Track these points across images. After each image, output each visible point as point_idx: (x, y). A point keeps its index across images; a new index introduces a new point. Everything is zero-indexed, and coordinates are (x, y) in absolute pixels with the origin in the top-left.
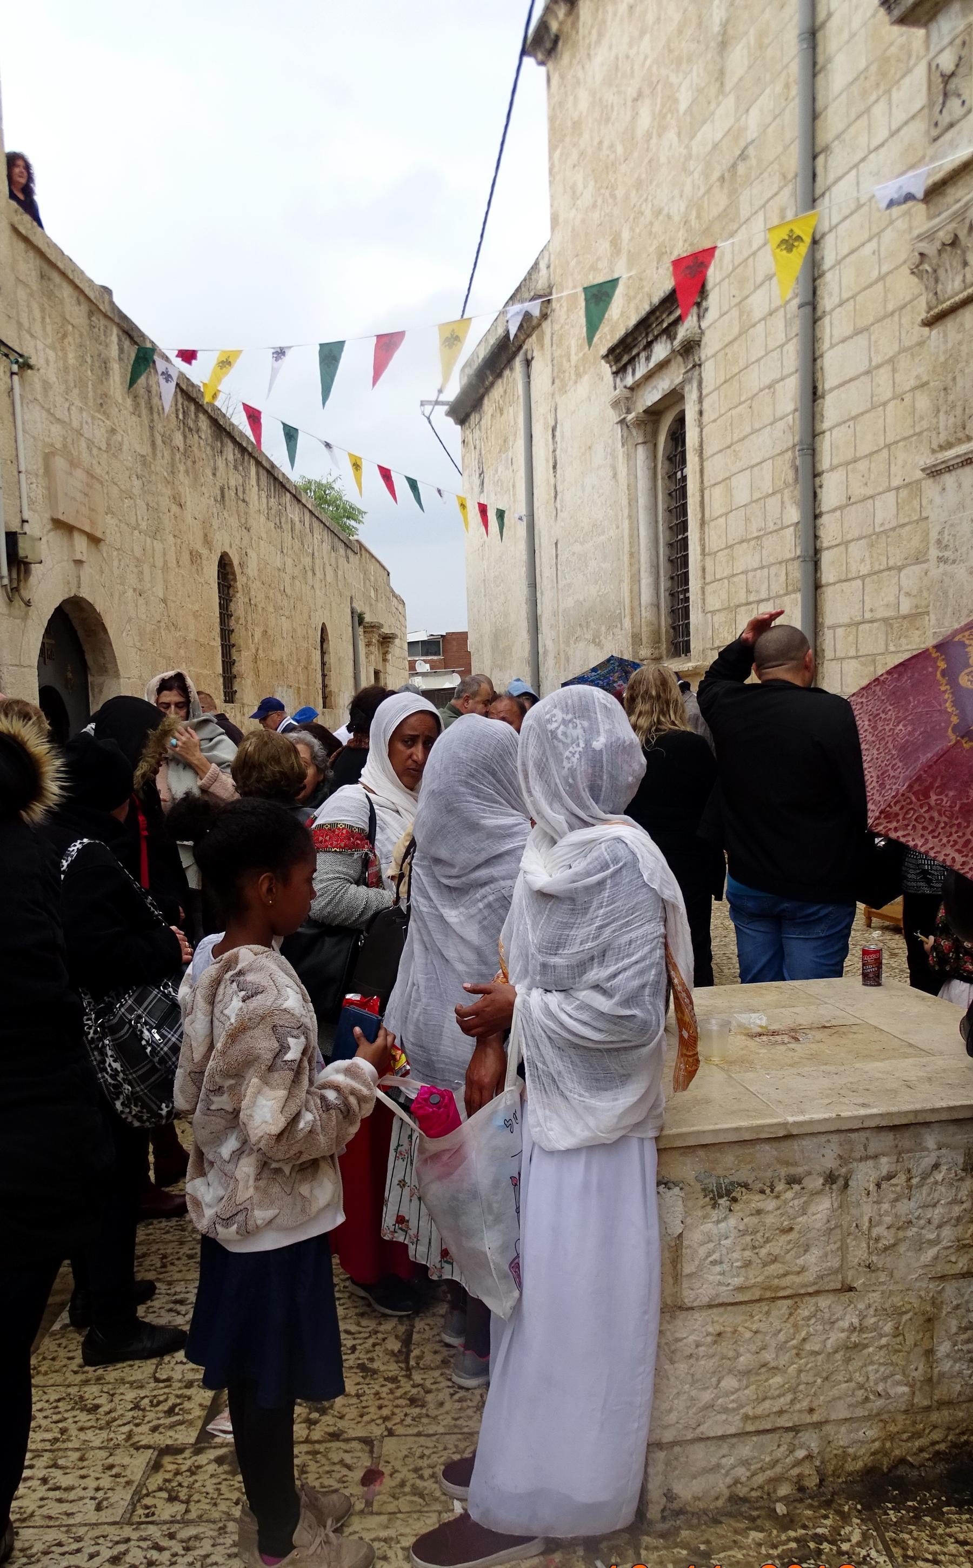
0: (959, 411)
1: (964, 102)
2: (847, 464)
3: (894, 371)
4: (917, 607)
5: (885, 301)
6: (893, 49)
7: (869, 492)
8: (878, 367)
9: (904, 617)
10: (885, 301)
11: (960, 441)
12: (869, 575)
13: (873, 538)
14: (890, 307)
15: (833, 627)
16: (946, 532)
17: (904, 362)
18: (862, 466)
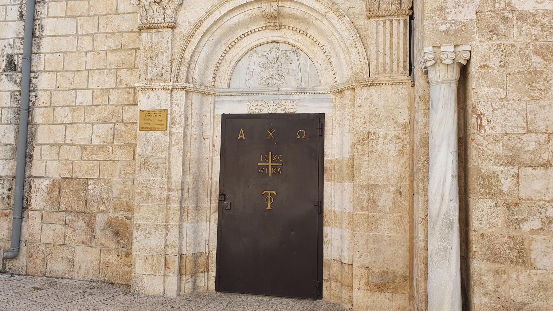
0: (159, 68)
2: (57, 72)
3: (93, 40)
4: (104, 142)
5: (89, 9)
7: (72, 87)
8: (82, 35)
9: (95, 145)
10: (89, 9)
12: (71, 124)
13: (74, 108)
14: (92, 13)
15: (41, 144)
17: (100, 37)
18: (70, 75)
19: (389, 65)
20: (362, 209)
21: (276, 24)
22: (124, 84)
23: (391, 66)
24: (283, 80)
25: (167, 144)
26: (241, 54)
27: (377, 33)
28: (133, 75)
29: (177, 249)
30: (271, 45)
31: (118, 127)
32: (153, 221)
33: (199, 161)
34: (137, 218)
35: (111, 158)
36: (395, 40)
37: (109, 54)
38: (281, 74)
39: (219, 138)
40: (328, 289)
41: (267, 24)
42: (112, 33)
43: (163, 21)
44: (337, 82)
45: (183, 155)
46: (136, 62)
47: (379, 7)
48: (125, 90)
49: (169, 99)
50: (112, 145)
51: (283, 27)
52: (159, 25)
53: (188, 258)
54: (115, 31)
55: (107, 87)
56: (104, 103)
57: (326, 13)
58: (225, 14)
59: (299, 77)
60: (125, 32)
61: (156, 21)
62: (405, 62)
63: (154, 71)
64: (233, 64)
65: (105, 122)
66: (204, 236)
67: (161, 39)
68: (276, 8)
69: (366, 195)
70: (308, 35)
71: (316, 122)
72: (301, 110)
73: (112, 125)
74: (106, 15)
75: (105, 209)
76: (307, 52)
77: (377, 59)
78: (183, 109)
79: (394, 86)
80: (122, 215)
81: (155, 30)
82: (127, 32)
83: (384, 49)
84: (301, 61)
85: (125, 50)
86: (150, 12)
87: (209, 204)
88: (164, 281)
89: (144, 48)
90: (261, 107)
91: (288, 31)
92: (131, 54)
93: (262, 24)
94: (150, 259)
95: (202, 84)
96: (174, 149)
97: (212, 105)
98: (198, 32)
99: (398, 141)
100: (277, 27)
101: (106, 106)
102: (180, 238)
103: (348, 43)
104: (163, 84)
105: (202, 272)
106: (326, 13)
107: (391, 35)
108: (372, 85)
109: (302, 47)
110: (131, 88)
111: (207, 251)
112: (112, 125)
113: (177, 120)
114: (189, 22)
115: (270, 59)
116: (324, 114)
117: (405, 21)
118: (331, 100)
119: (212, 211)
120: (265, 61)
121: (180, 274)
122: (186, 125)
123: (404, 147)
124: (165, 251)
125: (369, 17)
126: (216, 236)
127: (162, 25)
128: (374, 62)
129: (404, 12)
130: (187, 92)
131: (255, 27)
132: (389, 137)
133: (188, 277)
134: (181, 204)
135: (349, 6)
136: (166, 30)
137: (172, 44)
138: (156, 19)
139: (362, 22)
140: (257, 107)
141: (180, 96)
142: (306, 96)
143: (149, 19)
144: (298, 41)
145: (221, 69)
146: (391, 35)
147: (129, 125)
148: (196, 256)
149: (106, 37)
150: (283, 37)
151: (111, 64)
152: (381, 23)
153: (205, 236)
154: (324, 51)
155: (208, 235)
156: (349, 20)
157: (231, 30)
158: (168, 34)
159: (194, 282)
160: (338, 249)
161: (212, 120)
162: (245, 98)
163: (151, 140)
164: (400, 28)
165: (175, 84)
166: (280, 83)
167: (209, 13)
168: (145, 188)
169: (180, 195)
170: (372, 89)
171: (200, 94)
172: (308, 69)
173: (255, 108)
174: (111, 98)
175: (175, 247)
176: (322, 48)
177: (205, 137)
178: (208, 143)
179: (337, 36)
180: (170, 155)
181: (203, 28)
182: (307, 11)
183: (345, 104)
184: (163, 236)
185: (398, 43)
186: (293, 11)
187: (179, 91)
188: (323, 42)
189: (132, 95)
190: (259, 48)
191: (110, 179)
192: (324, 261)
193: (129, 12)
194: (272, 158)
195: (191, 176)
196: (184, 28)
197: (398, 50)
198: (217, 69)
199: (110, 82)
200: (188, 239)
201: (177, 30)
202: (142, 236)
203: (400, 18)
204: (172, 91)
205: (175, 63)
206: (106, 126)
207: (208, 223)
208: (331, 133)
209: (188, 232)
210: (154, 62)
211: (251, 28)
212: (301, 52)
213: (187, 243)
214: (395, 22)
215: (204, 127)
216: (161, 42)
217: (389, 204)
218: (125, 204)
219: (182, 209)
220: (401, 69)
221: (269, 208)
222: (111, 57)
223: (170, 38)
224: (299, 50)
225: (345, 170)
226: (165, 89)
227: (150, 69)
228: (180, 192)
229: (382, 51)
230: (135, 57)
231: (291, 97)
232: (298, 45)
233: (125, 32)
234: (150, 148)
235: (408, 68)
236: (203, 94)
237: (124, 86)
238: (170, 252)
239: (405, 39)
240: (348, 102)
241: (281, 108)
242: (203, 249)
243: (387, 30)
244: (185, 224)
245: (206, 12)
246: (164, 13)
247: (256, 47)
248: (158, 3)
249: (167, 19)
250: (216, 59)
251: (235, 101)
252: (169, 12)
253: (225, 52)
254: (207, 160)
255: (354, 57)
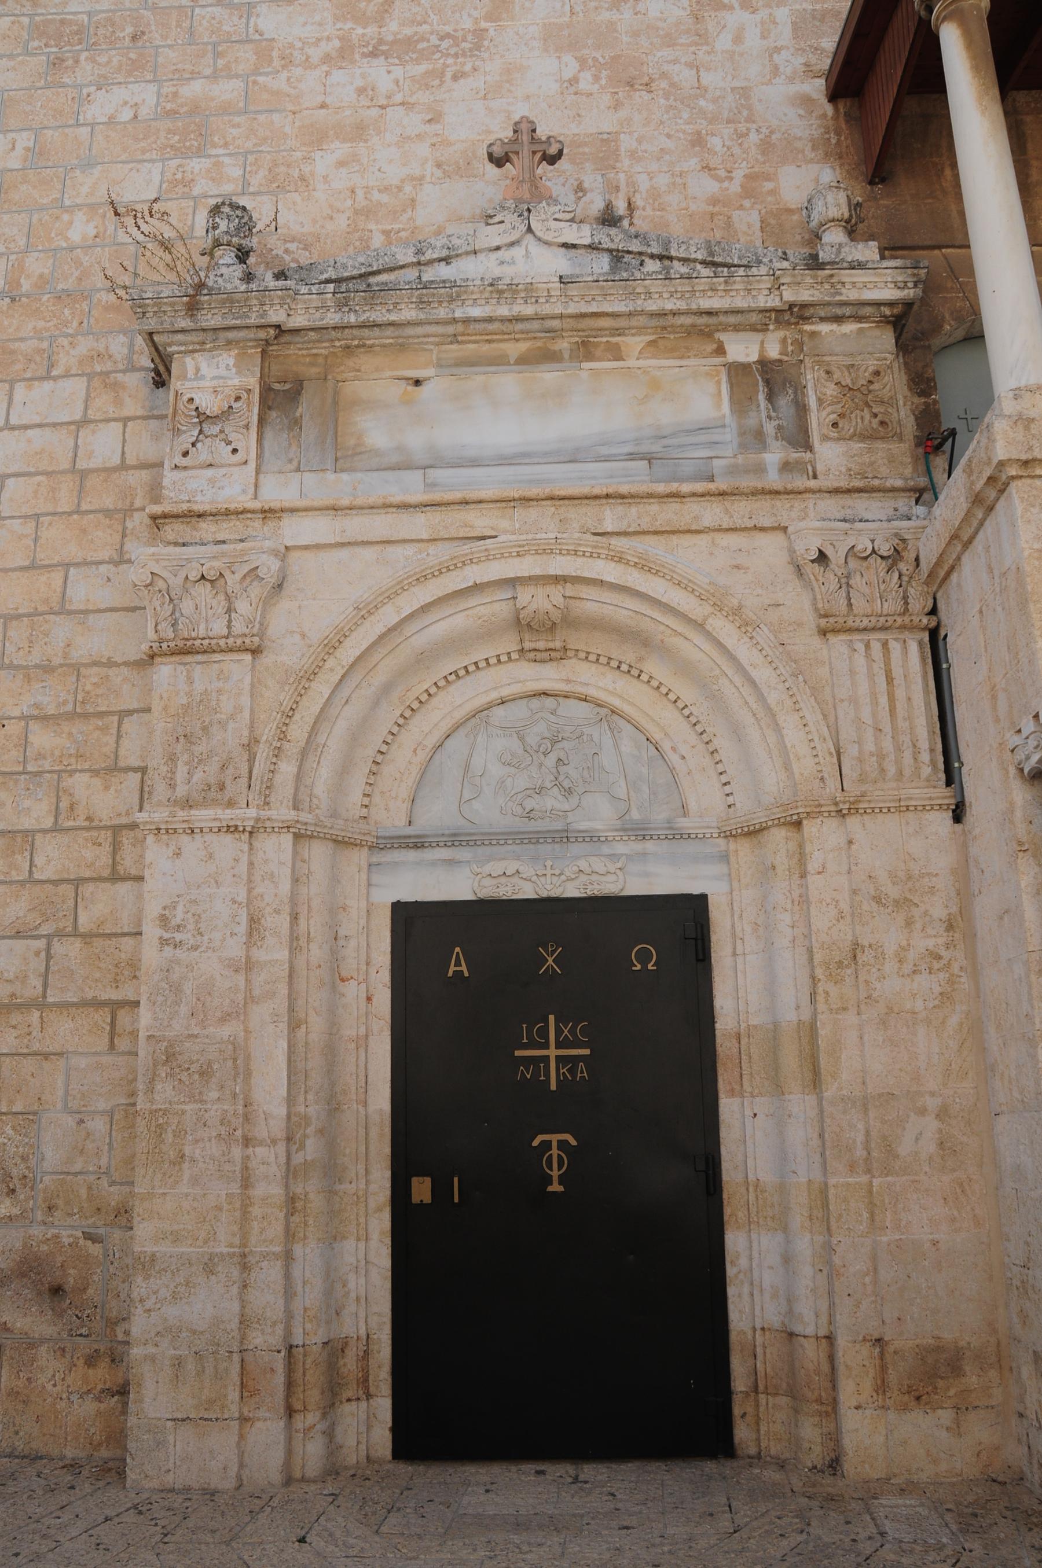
0: (213, 767)
1: (235, 451)
4: (13, 995)
6: (22, 346)
11: (215, 802)
16: (180, 908)
19: (892, 757)
20: (852, 1167)
21: (551, 645)
22: (82, 817)
23: (898, 762)
24: (574, 800)
25: (240, 997)
26: (445, 726)
27: (852, 672)
28: (112, 790)
29: (280, 1330)
30: (535, 703)
31: (58, 948)
32: (199, 1243)
33: (331, 1052)
34: (145, 1235)
35: (36, 1047)
36: (900, 693)
37: (33, 726)
38: (566, 784)
39: (386, 976)
40: (748, 1418)
41: (527, 645)
42: (48, 669)
43: (225, 632)
44: (738, 805)
45: (289, 1033)
46: (122, 752)
47: (850, 605)
48: (85, 834)
49: (245, 859)
50: (41, 1004)
51: (570, 654)
52: (214, 642)
53: (309, 1361)
54: (57, 661)
55: (27, 826)
56: (15, 876)
57: (706, 618)
58: (411, 616)
59: (621, 791)
60: (86, 666)
61: (202, 633)
62: (932, 750)
63: (198, 776)
64: (422, 755)
65: (18, 935)
66: (352, 1285)
67: (221, 684)
68: (559, 600)
69: (861, 1126)
70: (644, 677)
71: (684, 922)
72: (636, 886)
73: (41, 944)
74: (29, 615)
75: (16, 1211)
76: (643, 721)
77: (859, 742)
78: (285, 887)
79: (910, 815)
80: (73, 1227)
81: (199, 658)
82: (95, 664)
83: (874, 715)
84: (623, 749)
85: (86, 716)
86: (187, 606)
87: (362, 1186)
88: (241, 1437)
89: (165, 708)
90: (515, 880)
91: (585, 665)
92: (104, 730)
93: (509, 644)
94: (191, 1366)
95: (334, 815)
96: (260, 1013)
97: (364, 876)
98: (331, 662)
99: (936, 965)
100: (553, 654)
101: (22, 883)
102: (289, 1293)
103: (772, 698)
104: (227, 815)
105: (349, 1400)
106: (706, 618)
107: (890, 680)
108: (854, 810)
109: (627, 709)
110: (106, 827)
111: (362, 1332)
112: (41, 944)
113: (269, 921)
114: (303, 636)
115: (532, 740)
116: (703, 898)
117: (920, 643)
118: (725, 858)
119: (372, 1204)
120: (515, 745)
121: (290, 1412)
122: (294, 938)
123: (953, 983)
124: (243, 1338)
125: (823, 633)
126: (388, 1285)
127: (222, 642)
128: (851, 752)
129: (916, 620)
130: (297, 836)
131: (488, 651)
132: (911, 955)
133: (312, 1418)
134: (287, 1186)
135: (767, 602)
136: (235, 656)
137: (252, 696)
138: (202, 626)
139: (806, 642)
140: (503, 880)
141: (276, 849)
142: (650, 846)
143: (181, 626)
144: (612, 693)
145: (386, 770)
146: (890, 680)
147: (98, 943)
148: (334, 1349)
149: (28, 679)
150: (568, 681)
151: (40, 756)
152: (860, 647)
153: (355, 1284)
154: (693, 720)
155: (362, 1281)
156: (772, 638)
157: (423, 659)
158: (238, 667)
159: (330, 1434)
160: (775, 1296)
161: (363, 922)
162: (463, 854)
163: (188, 988)
164: (910, 658)
165: (262, 813)
166: (566, 807)
167: (365, 611)
168: (169, 1137)
169: (283, 1160)
170: (853, 821)
171: (331, 845)
172: (645, 770)
173: (495, 882)
174: (39, 860)
175: (274, 1324)
176: (686, 712)
177: (344, 974)
178: (352, 991)
179: (738, 680)
180: (247, 1031)
181: (349, 652)
182: (649, 612)
183: (774, 868)
184: (235, 1290)
185: (909, 699)
186: (608, 610)
187: (274, 836)
188: (687, 694)
189: (107, 848)
190: (499, 712)
191: (35, 1113)
192: (733, 1337)
193: (103, 606)
194: (559, 1032)
195: (311, 1097)
196: (287, 652)
197: (909, 718)
198: (375, 769)
199: (37, 812)
200: (310, 1297)
201: (267, 659)
202: (163, 1293)
203: (906, 635)
204: (251, 833)
205: (263, 753)
206: (19, 945)
207: (362, 1245)
208: (728, 950)
209: (308, 1274)
210: (197, 749)
211: (479, 656)
212: (622, 723)
213: (305, 1310)
214: (895, 647)
215: (341, 942)
216: (219, 691)
217: (929, 1147)
218: (83, 1192)
219: (292, 1204)
220: (926, 771)
221: (556, 1187)
222: (41, 738)
223: (248, 679)
224: (615, 717)
225: (790, 1059)
226: (232, 829)
227: (185, 769)
228: (281, 1148)
229: (870, 722)
230: (119, 736)
231: (606, 849)
232: (616, 702)
233: (86, 666)
234: (184, 1010)
235: (941, 766)
236: (341, 843)
237: (81, 822)
238: (258, 1341)
239: (926, 692)
240: (782, 860)
241: (576, 883)
242: (351, 1326)
243: (875, 666)
244: (298, 1250)
245: (357, 608)
246: (229, 610)
247: (489, 706)
248: (212, 582)
249: (238, 627)
250: (375, 740)
251: (433, 863)
252: (243, 607)
253: (401, 721)
254: (353, 1045)
255: (793, 736)
